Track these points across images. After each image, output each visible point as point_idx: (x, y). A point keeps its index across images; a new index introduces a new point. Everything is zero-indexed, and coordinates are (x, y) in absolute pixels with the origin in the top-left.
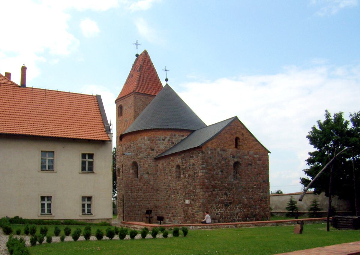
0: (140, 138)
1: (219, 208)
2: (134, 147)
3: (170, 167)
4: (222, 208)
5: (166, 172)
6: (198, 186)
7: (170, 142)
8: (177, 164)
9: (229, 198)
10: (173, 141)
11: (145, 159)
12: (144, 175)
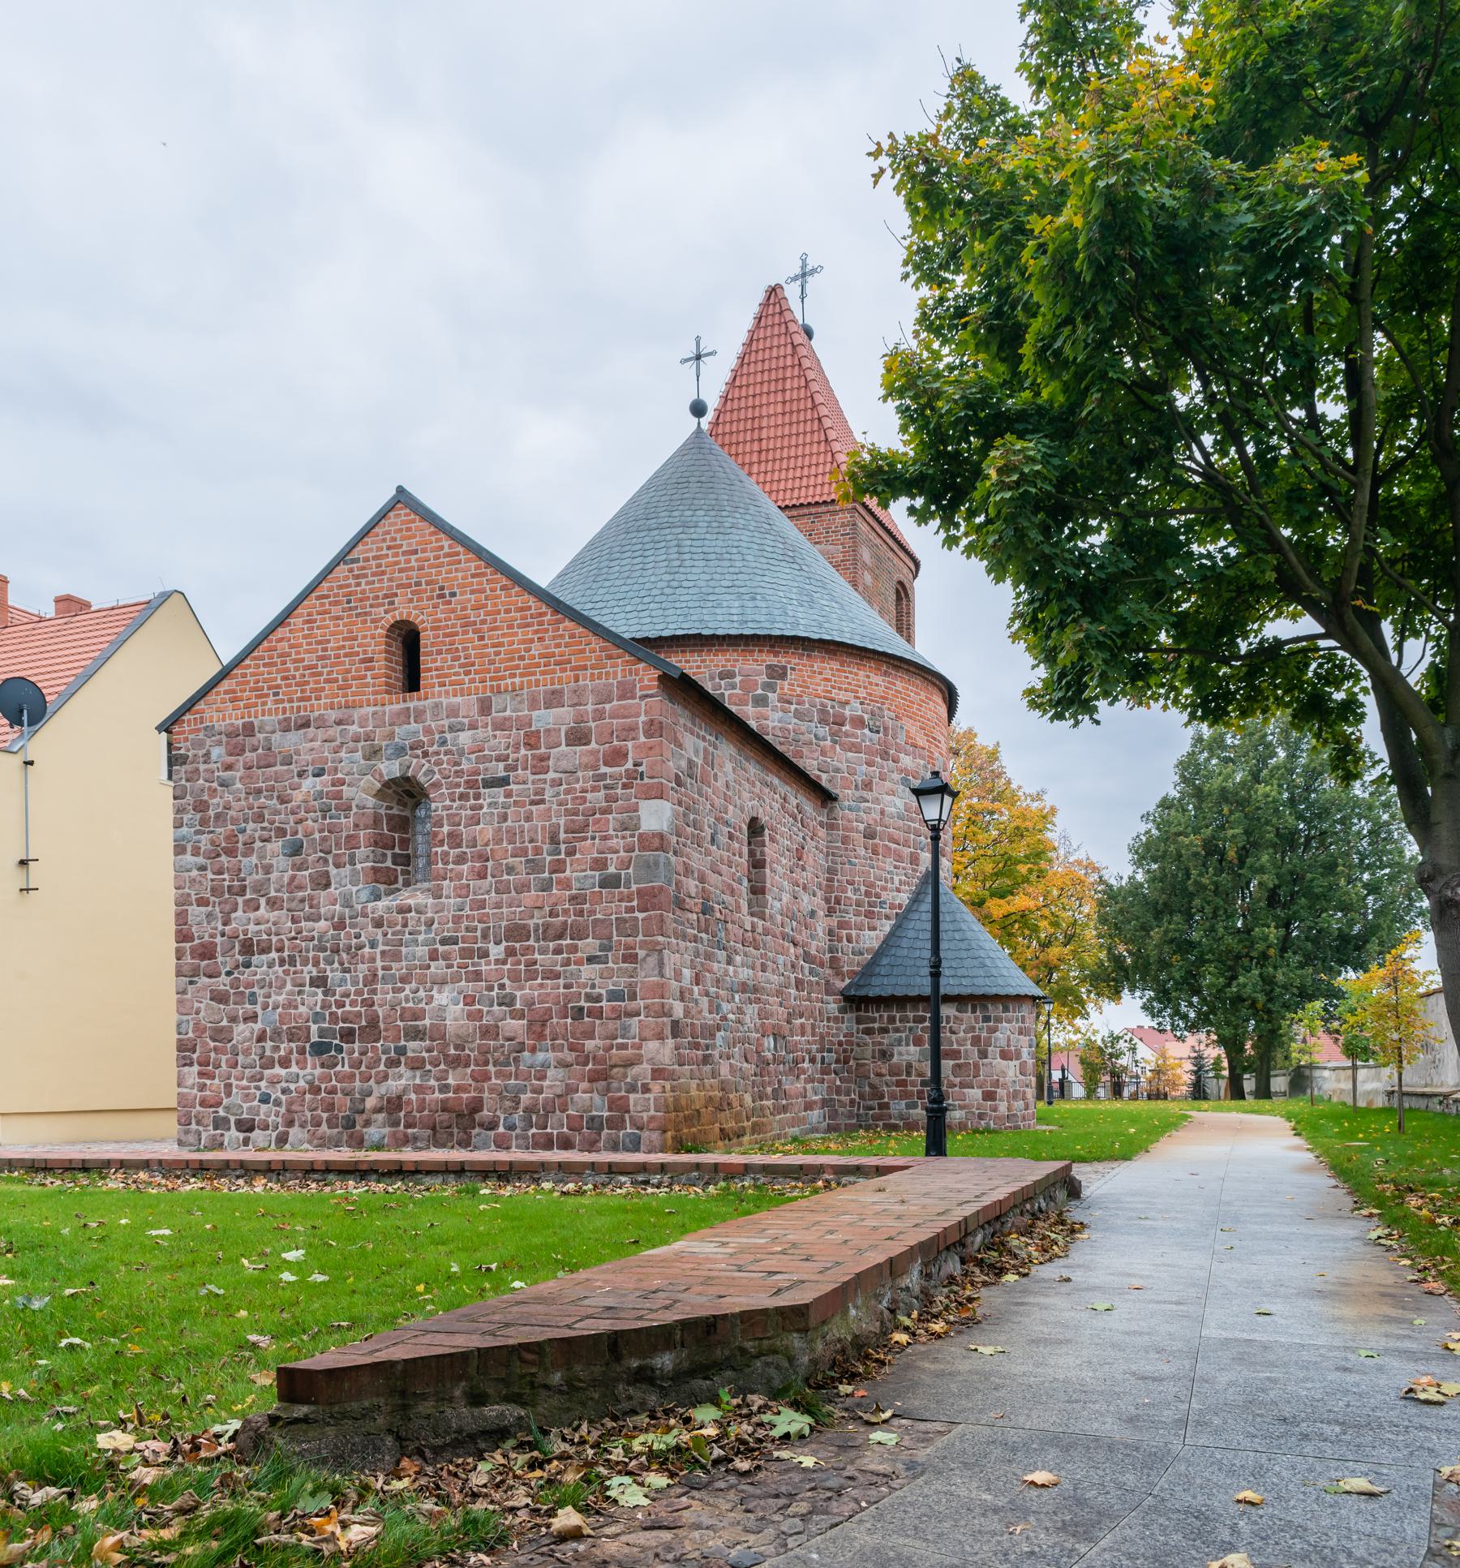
1: (285, 1063)
4: (302, 1065)
9: (340, 1005)
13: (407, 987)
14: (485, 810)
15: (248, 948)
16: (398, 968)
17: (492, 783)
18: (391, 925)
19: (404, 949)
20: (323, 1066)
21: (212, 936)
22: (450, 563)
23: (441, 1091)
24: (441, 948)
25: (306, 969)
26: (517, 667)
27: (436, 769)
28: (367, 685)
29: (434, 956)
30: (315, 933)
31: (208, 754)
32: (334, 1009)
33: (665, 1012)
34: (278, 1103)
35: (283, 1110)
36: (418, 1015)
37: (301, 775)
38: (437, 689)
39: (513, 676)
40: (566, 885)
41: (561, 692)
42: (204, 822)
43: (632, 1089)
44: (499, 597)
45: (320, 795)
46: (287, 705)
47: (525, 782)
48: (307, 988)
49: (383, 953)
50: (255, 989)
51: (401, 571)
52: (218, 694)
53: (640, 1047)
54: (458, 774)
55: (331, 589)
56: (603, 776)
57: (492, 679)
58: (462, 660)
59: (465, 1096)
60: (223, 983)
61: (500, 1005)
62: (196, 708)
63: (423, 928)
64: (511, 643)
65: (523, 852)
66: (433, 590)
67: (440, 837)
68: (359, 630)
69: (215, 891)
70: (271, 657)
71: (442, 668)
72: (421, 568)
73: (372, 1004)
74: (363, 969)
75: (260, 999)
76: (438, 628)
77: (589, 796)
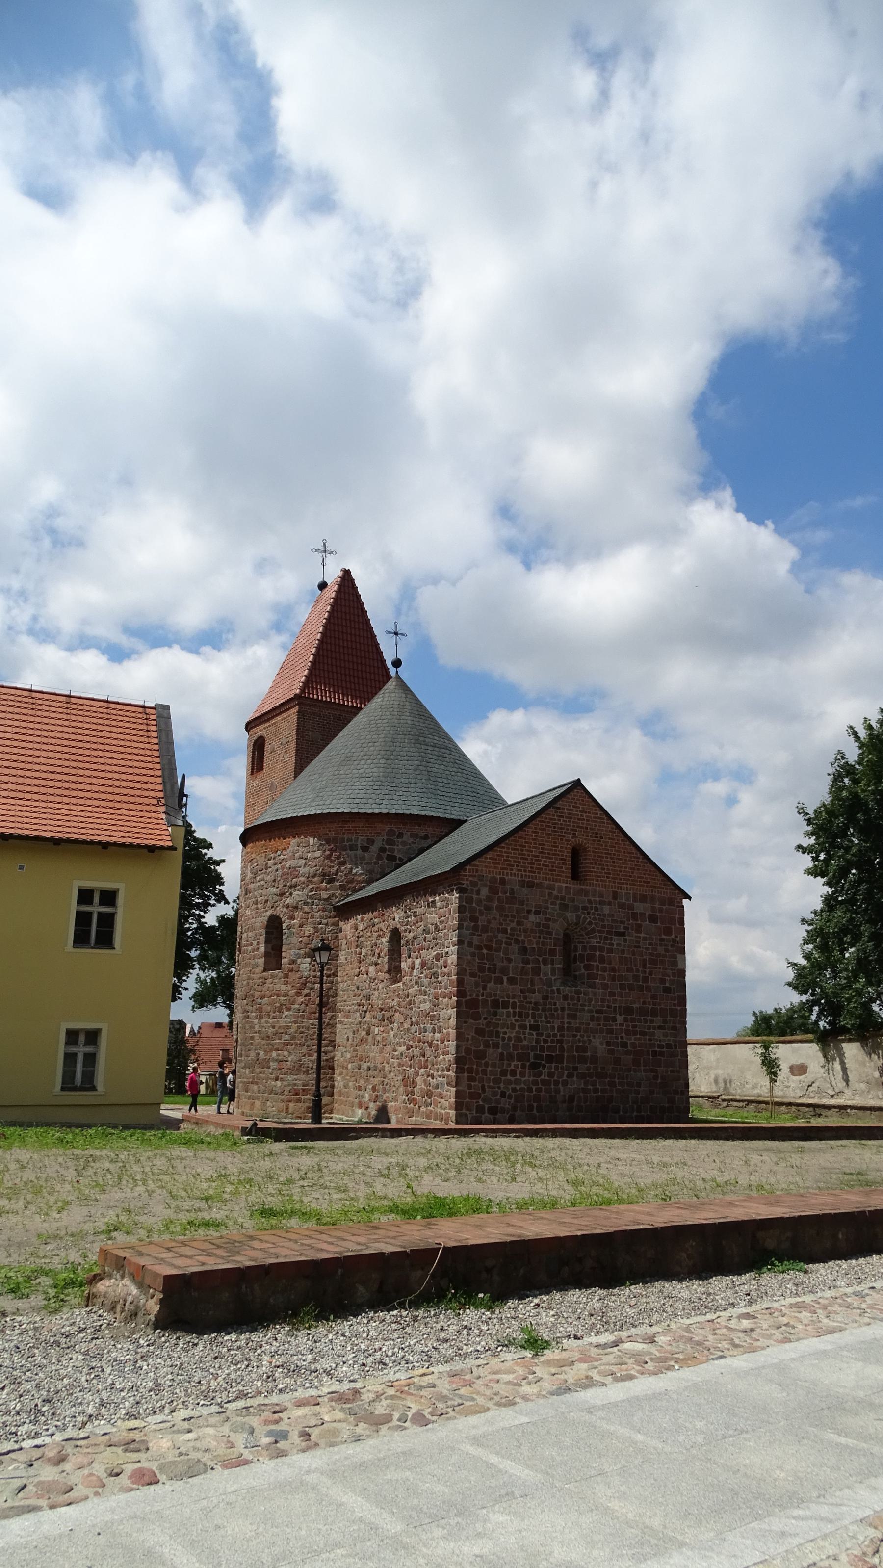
0: (294, 842)
2: (277, 870)
3: (375, 934)
4: (522, 1074)
5: (364, 951)
6: (444, 998)
7: (384, 855)
8: (392, 924)
9: (545, 1041)
10: (395, 854)
11: (306, 909)
12: (299, 961)
15: (496, 1004)
18: (572, 999)
21: (477, 995)
23: (594, 1092)
30: (533, 1000)
34: (510, 1097)
35: (512, 1101)
36: (585, 1050)
37: (529, 912)
40: (649, 989)
42: (476, 928)
45: (538, 925)
52: (486, 858)
54: (604, 926)
56: (662, 940)
60: (482, 1023)
62: (474, 863)
69: (481, 969)
70: (515, 845)
74: (557, 1024)
75: (501, 1035)
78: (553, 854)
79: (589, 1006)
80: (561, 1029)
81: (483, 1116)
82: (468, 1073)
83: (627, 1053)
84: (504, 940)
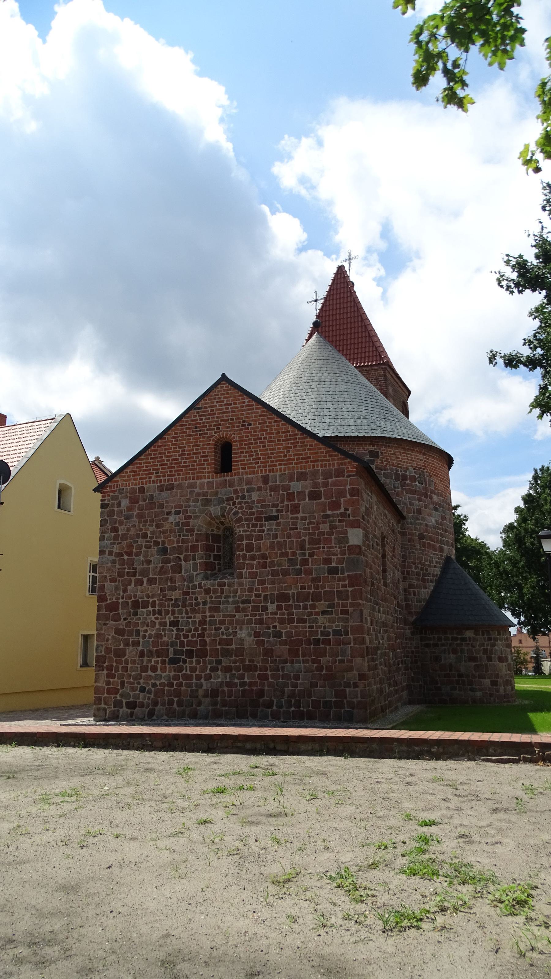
4: (164, 670)
13: (223, 627)
14: (265, 532)
15: (136, 605)
16: (219, 617)
17: (268, 519)
18: (215, 591)
19: (221, 606)
20: (175, 671)
22: (248, 410)
24: (242, 606)
25: (167, 617)
26: (283, 460)
27: (240, 511)
28: (205, 468)
29: (238, 610)
30: (173, 598)
31: (120, 503)
32: (182, 639)
33: (363, 642)
34: (149, 692)
35: (152, 696)
36: (229, 642)
37: (168, 513)
38: (241, 471)
39: (281, 465)
41: (305, 473)
42: (116, 538)
43: (348, 685)
44: (273, 426)
45: (177, 524)
46: (162, 478)
47: (286, 519)
48: (168, 627)
49: (210, 608)
50: (139, 628)
51: (223, 413)
53: (352, 662)
54: (252, 514)
55: (187, 421)
56: (328, 516)
57: (269, 466)
58: (254, 457)
59: (254, 688)
60: (122, 624)
61: (274, 637)
62: (115, 479)
63: (232, 595)
64: (280, 449)
65: (286, 554)
66: (239, 423)
67: (242, 547)
68: (200, 442)
69: (121, 575)
70: (155, 454)
71: (244, 460)
72: (234, 412)
73: (204, 637)
74: (198, 617)
75: (142, 633)
76: (242, 441)
77: (321, 526)
78: (194, 454)
79: (234, 597)
80: (203, 622)
81: (121, 710)
82: (107, 670)
83: (284, 643)
84: (144, 544)
